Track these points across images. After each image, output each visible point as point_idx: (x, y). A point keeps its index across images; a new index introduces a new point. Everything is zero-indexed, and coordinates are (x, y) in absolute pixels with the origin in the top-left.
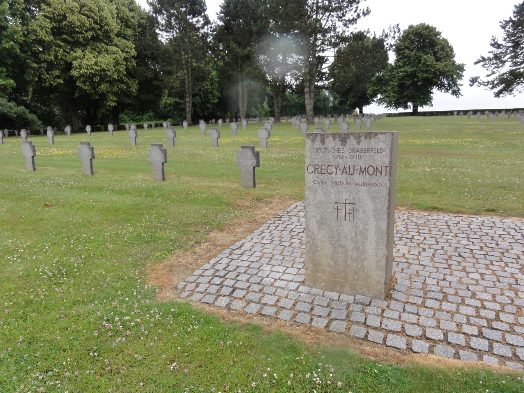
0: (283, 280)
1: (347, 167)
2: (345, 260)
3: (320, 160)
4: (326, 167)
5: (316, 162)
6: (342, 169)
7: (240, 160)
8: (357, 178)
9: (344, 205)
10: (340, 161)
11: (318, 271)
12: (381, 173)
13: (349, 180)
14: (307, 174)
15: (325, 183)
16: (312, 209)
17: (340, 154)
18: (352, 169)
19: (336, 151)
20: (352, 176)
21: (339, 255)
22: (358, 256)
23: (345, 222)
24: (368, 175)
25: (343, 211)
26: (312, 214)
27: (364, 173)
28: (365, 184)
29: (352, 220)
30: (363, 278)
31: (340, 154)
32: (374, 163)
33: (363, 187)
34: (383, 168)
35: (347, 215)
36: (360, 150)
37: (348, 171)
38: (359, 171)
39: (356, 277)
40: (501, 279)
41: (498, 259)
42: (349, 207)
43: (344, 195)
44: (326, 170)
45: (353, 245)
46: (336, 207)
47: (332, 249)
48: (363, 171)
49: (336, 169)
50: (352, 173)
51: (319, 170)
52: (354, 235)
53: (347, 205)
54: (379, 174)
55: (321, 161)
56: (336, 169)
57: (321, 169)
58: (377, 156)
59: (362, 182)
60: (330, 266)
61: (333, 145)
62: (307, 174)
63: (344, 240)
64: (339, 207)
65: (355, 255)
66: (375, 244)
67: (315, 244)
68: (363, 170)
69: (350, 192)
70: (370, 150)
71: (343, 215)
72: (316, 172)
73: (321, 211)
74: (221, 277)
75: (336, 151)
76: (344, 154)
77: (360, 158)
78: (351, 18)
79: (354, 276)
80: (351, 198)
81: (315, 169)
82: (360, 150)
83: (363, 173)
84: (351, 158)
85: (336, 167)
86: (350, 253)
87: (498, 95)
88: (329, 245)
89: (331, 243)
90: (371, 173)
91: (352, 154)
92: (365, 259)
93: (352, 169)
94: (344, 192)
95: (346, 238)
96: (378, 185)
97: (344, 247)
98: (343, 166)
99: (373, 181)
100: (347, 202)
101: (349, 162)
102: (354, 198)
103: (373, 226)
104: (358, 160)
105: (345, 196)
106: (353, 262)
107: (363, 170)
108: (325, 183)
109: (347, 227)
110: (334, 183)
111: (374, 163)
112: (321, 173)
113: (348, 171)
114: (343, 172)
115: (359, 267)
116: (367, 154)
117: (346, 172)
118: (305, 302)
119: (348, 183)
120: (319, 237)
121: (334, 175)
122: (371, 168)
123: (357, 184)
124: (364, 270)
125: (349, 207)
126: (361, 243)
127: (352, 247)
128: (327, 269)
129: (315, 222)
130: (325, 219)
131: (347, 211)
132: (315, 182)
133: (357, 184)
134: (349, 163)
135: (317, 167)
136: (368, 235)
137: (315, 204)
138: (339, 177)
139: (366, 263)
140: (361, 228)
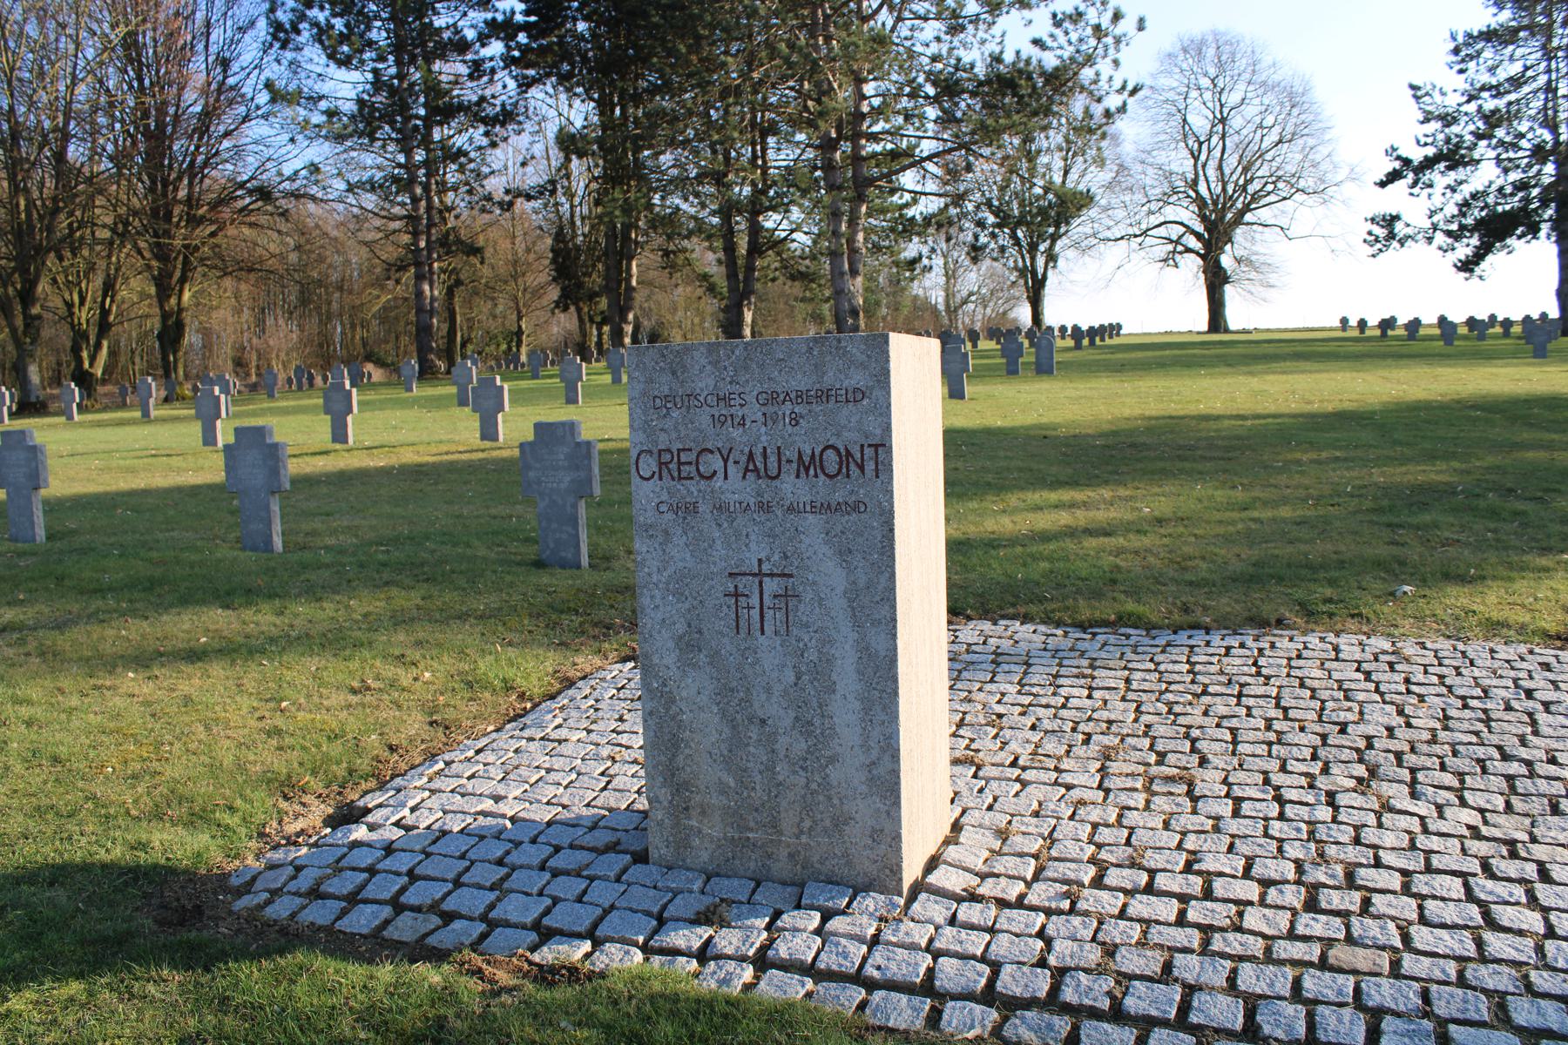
0: (582, 848)
1: (758, 452)
2: (770, 768)
3: (674, 435)
4: (692, 457)
5: (663, 441)
6: (744, 458)
7: (532, 474)
8: (792, 487)
9: (757, 580)
10: (736, 433)
11: (687, 809)
12: (861, 467)
13: (767, 497)
14: (635, 480)
15: (691, 509)
16: (658, 601)
17: (733, 410)
18: (773, 459)
19: (722, 404)
20: (777, 483)
21: (752, 749)
22: (808, 752)
23: (762, 639)
24: (822, 477)
25: (755, 601)
26: (659, 616)
27: (812, 472)
28: (815, 508)
29: (783, 631)
30: (828, 823)
31: (733, 410)
32: (838, 435)
33: (811, 517)
34: (867, 450)
35: (769, 614)
36: (793, 395)
37: (760, 466)
38: (795, 465)
39: (807, 824)
40: (1290, 811)
41: (1307, 753)
42: (771, 586)
43: (753, 546)
44: (693, 468)
45: (792, 714)
46: (732, 589)
47: (727, 731)
48: (808, 465)
49: (726, 461)
50: (774, 472)
51: (673, 466)
52: (793, 679)
53: (766, 579)
54: (858, 471)
55: (679, 438)
56: (726, 461)
57: (680, 463)
58: (845, 412)
59: (807, 499)
60: (723, 790)
61: (711, 382)
62: (635, 480)
63: (763, 697)
64: (741, 588)
65: (801, 746)
66: (857, 705)
67: (673, 718)
68: (807, 459)
69: (772, 535)
70: (824, 395)
71: (755, 613)
72: (665, 473)
73: (687, 605)
74: (492, 889)
75: (722, 404)
76: (745, 410)
77: (795, 421)
78: (922, 12)
79: (802, 820)
80: (776, 557)
81: (661, 464)
82: (793, 395)
83: (807, 470)
84: (770, 423)
85: (725, 453)
86: (783, 741)
87: (1467, 266)
88: (717, 719)
89: (723, 713)
90: (832, 469)
91: (770, 409)
92: (833, 760)
93: (773, 459)
94: (753, 537)
95: (768, 690)
96: (856, 507)
97: (763, 722)
98: (747, 450)
99: (839, 497)
100: (766, 568)
101: (764, 437)
102: (786, 557)
103: (847, 647)
104: (789, 428)
105: (755, 551)
106: (794, 772)
107: (807, 459)
108: (691, 509)
109: (770, 653)
110: (721, 508)
111: (838, 435)
112: (680, 478)
113: (760, 466)
114: (747, 470)
115: (814, 786)
116: (817, 408)
117: (756, 470)
118: (636, 912)
119: (764, 507)
120: (684, 694)
121: (718, 482)
122: (830, 452)
123: (790, 509)
124: (830, 798)
125: (771, 586)
126: (815, 705)
127: (788, 722)
128: (715, 800)
129: (671, 644)
130: (700, 632)
131: (767, 601)
132: (663, 508)
133: (790, 509)
134: (763, 438)
135: (667, 457)
136: (834, 677)
137: (668, 583)
138: (736, 488)
139: (835, 774)
140: (812, 655)
